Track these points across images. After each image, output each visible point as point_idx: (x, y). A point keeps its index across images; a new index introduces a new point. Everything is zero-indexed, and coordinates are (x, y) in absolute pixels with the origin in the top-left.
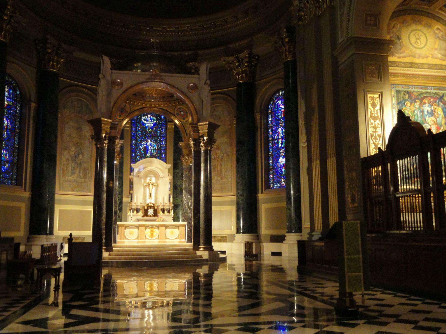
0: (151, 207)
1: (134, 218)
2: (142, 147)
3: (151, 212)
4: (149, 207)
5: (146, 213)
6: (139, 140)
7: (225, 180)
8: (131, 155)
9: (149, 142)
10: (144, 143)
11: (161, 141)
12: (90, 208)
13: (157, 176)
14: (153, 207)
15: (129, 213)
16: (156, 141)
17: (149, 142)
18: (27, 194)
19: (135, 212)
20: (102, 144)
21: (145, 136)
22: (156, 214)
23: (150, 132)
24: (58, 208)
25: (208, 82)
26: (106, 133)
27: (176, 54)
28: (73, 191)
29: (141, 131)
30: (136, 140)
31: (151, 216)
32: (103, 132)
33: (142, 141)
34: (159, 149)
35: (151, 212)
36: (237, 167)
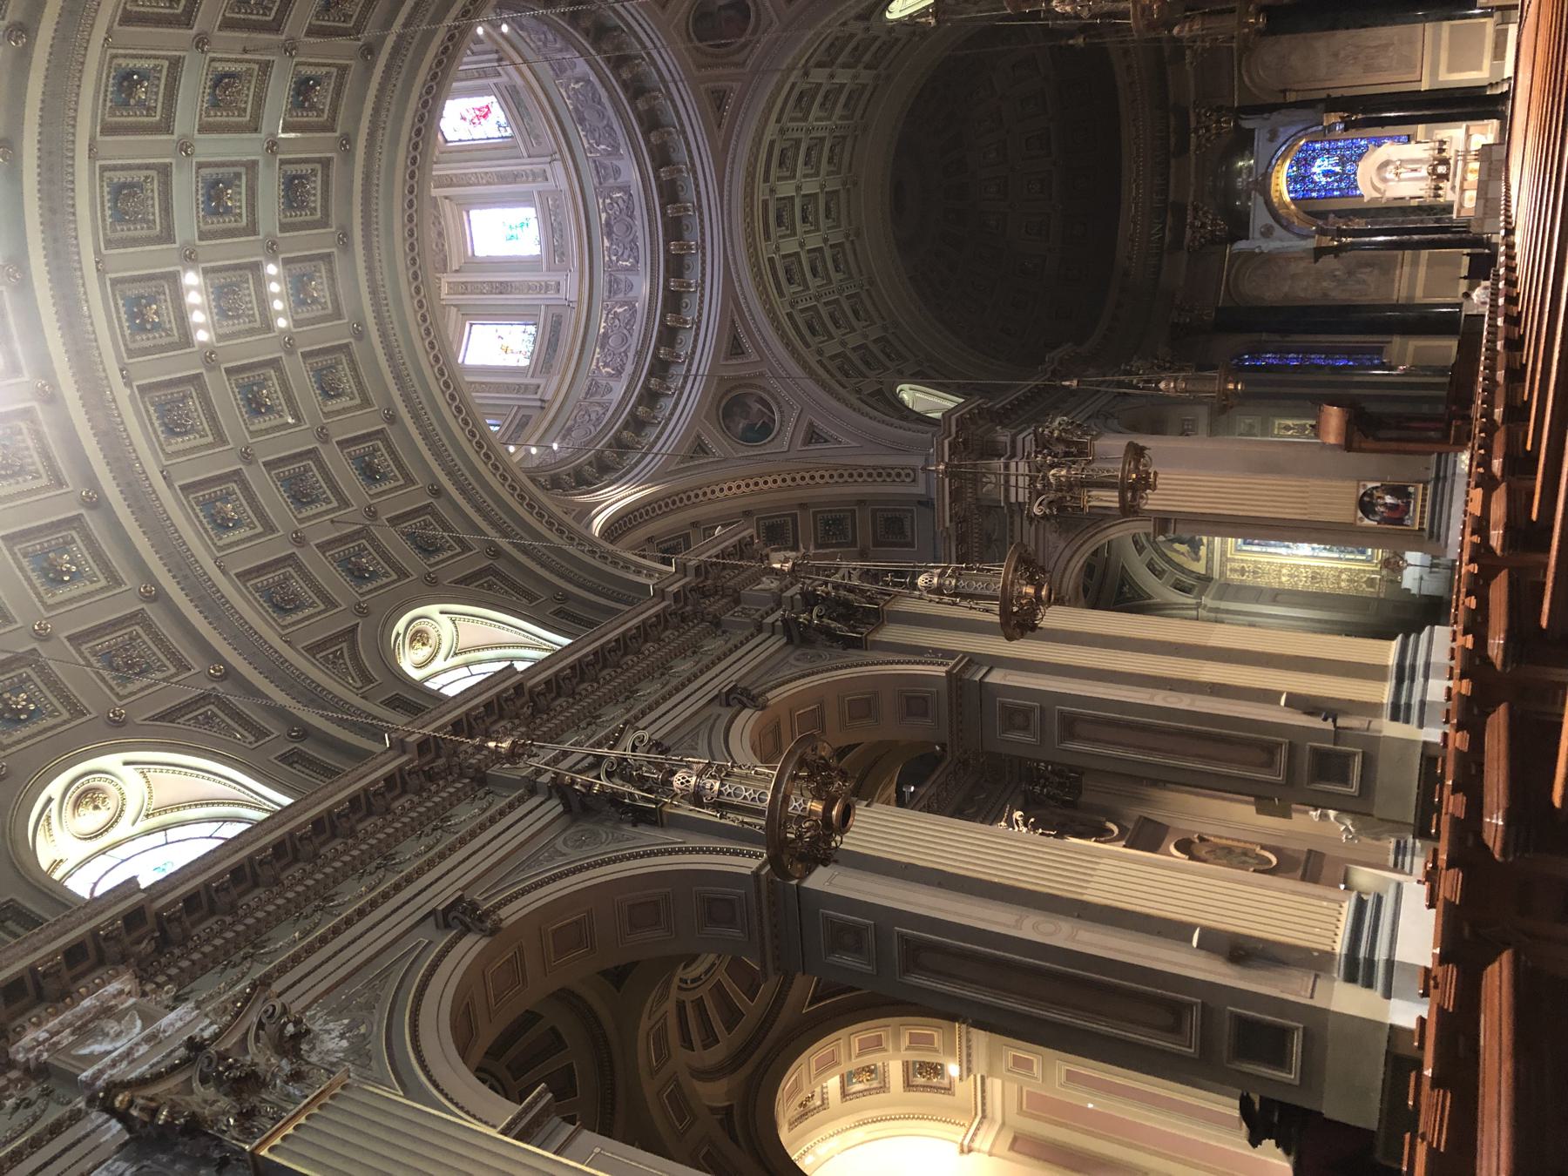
0: (1434, 169)
1: (1450, 193)
2: (1324, 181)
3: (1441, 169)
4: (1433, 172)
5: (1445, 177)
6: (1311, 186)
7: (1396, 38)
8: (1336, 197)
9: (1314, 170)
10: (1316, 178)
11: (1314, 150)
12: (1425, 253)
13: (1385, 164)
14: (1434, 168)
15: (1442, 200)
16: (1314, 158)
17: (1314, 170)
18: (1397, 340)
19: (1440, 192)
20: (1347, 245)
21: (1304, 178)
22: (1445, 162)
23: (1298, 168)
24: (1420, 296)
25: (1266, 115)
26: (1333, 240)
27: (1173, 140)
28: (1393, 281)
29: (1296, 183)
30: (1312, 190)
31: (1449, 169)
32: (1331, 244)
33: (1313, 182)
34: (1328, 151)
35: (1441, 169)
36: (1376, 26)
